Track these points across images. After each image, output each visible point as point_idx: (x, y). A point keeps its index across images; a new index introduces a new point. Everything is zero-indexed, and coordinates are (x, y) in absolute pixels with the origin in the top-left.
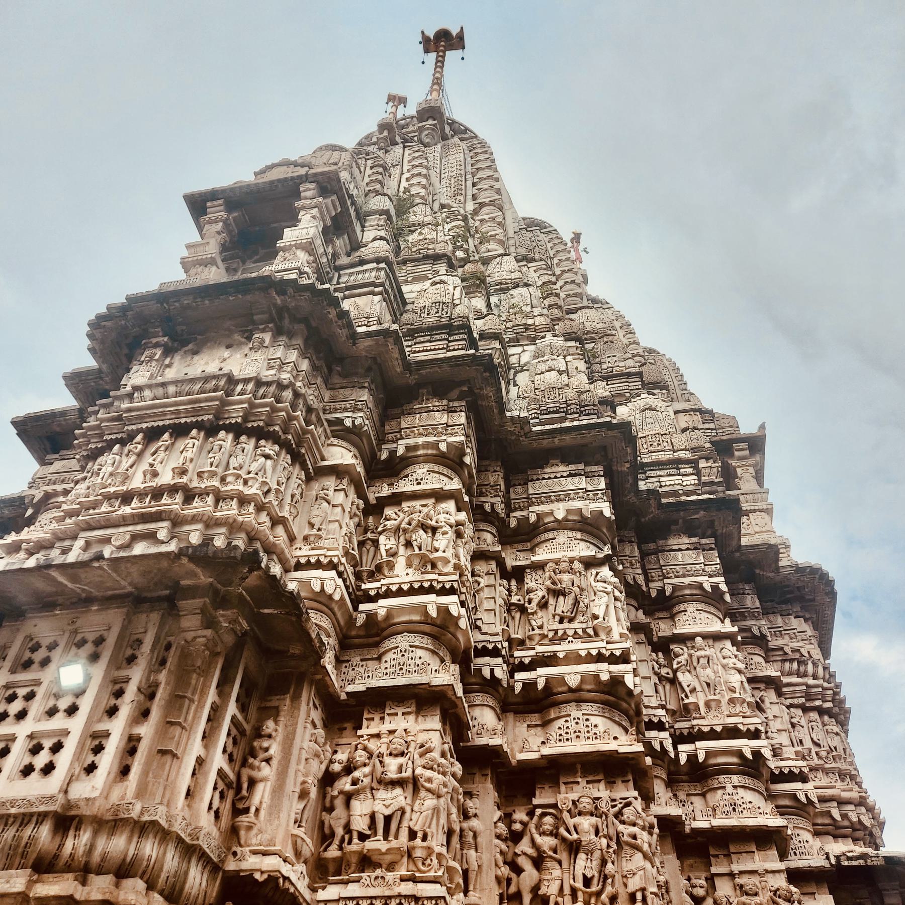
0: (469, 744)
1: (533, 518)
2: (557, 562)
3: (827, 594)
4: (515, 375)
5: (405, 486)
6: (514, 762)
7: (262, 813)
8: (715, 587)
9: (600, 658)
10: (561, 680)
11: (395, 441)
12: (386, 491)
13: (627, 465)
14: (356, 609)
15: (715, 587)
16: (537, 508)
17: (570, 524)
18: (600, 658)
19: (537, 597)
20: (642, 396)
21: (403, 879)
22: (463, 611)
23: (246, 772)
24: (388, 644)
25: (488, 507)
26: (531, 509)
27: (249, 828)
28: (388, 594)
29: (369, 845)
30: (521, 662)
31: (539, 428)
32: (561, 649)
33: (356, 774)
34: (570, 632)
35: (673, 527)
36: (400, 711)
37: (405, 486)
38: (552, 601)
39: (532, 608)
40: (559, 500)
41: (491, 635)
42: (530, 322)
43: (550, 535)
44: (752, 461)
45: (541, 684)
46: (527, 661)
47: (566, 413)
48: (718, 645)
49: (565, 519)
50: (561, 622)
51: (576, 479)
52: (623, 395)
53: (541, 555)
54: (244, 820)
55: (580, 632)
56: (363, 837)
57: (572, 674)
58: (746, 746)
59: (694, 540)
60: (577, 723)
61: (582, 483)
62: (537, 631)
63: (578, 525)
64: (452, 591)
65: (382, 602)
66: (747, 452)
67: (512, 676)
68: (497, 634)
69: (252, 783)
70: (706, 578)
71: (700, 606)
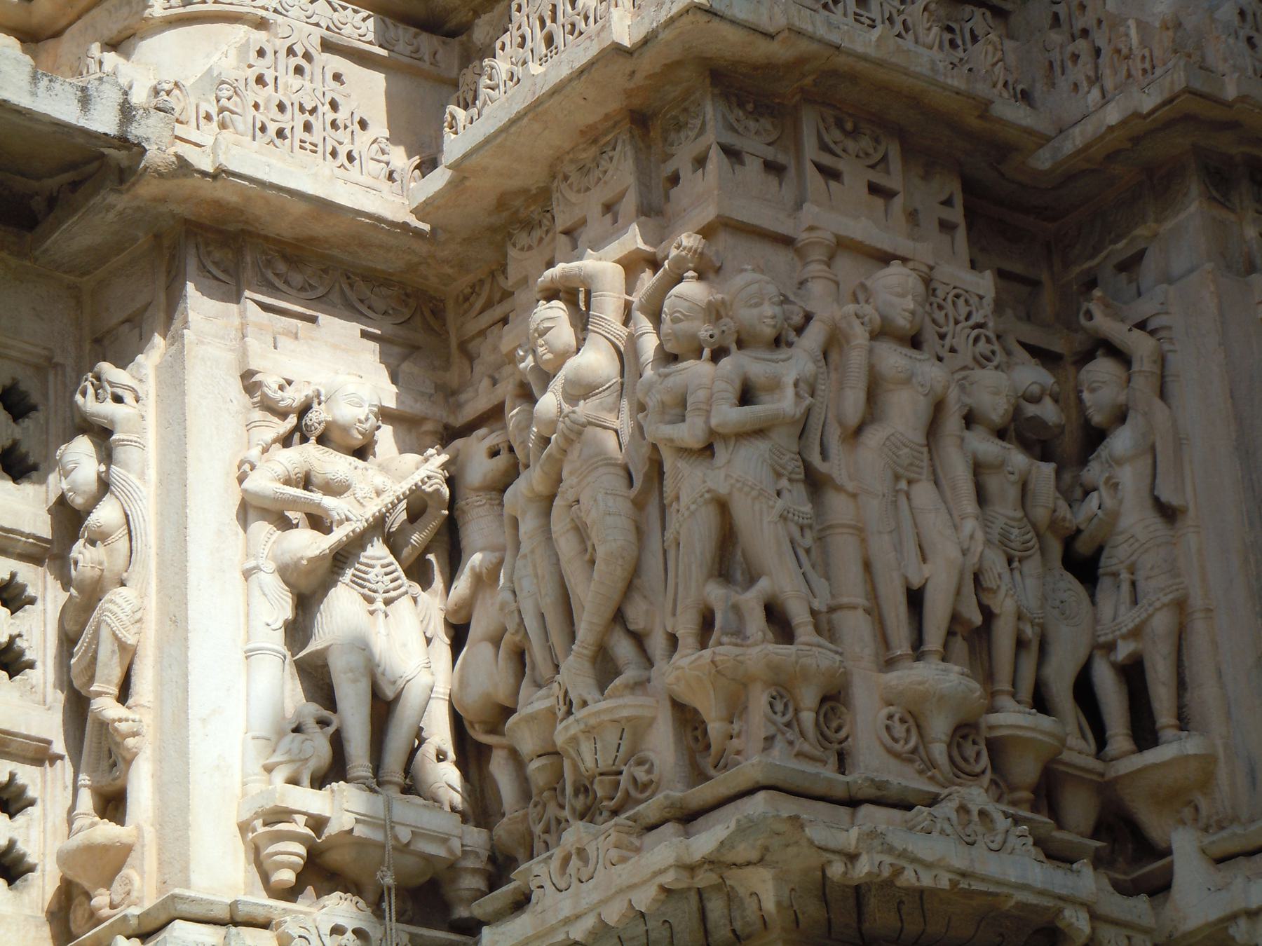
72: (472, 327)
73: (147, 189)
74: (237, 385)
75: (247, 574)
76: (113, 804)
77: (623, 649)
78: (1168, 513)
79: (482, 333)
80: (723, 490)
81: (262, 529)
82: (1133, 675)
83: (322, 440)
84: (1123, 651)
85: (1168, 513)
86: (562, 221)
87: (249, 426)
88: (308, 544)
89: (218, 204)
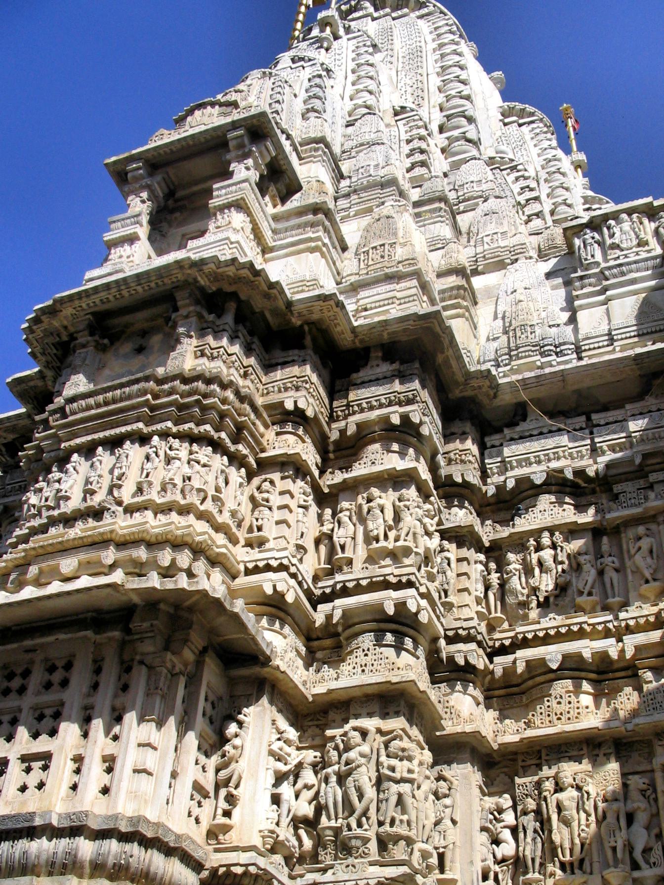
0: (444, 733)
5: (359, 470)
6: (495, 747)
10: (542, 662)
11: (345, 417)
12: (339, 477)
14: (315, 610)
21: (372, 864)
22: (424, 603)
28: (345, 592)
30: (503, 645)
37: (359, 470)
41: (465, 620)
45: (521, 668)
46: (507, 643)
57: (552, 654)
60: (559, 703)
64: (410, 584)
67: (491, 662)
68: (472, 619)
72: (306, 723)
73: (266, 670)
74: (270, 722)
75: (267, 769)
76: (227, 814)
77: (364, 819)
78: (454, 822)
79: (310, 727)
80: (402, 792)
81: (271, 758)
82: (441, 857)
83: (285, 742)
84: (441, 850)
85: (454, 822)
86: (352, 711)
87: (272, 733)
88: (284, 768)
89: (277, 678)
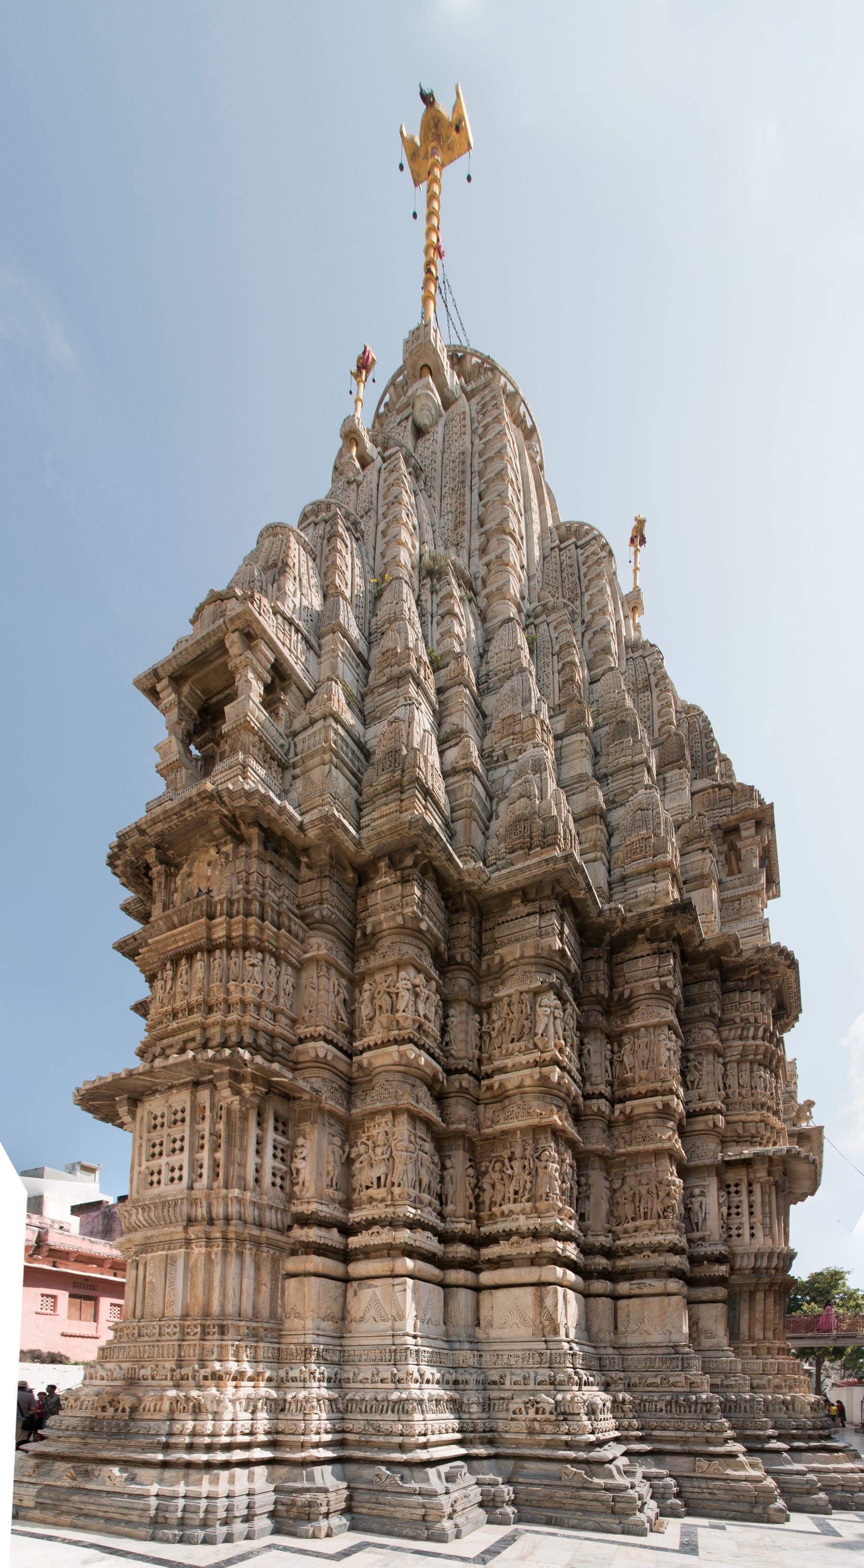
1: (497, 960)
2: (510, 996)
3: (789, 967)
4: (498, 805)
7: (306, 1184)
8: (663, 986)
9: (536, 1064)
13: (583, 892)
15: (663, 986)
16: (500, 951)
17: (526, 960)
18: (536, 1064)
19: (497, 1025)
20: (640, 792)
23: (293, 1166)
24: (375, 1081)
25: (459, 959)
26: (496, 952)
27: (301, 1191)
28: (369, 1048)
29: (370, 1191)
31: (497, 874)
32: (509, 1062)
33: (361, 1159)
34: (517, 1049)
35: (640, 936)
36: (383, 1120)
38: (508, 1026)
39: (494, 1034)
40: (517, 940)
42: (517, 728)
43: (512, 971)
44: (758, 838)
47: (530, 849)
48: (658, 1031)
49: (522, 957)
50: (512, 1041)
51: (532, 918)
52: (625, 792)
53: (503, 992)
54: (297, 1189)
55: (523, 1048)
56: (368, 1188)
58: (658, 1100)
59: (655, 945)
61: (535, 921)
62: (497, 1050)
63: (533, 960)
65: (365, 1055)
66: (752, 831)
69: (298, 1171)
70: (657, 979)
71: (650, 1002)
